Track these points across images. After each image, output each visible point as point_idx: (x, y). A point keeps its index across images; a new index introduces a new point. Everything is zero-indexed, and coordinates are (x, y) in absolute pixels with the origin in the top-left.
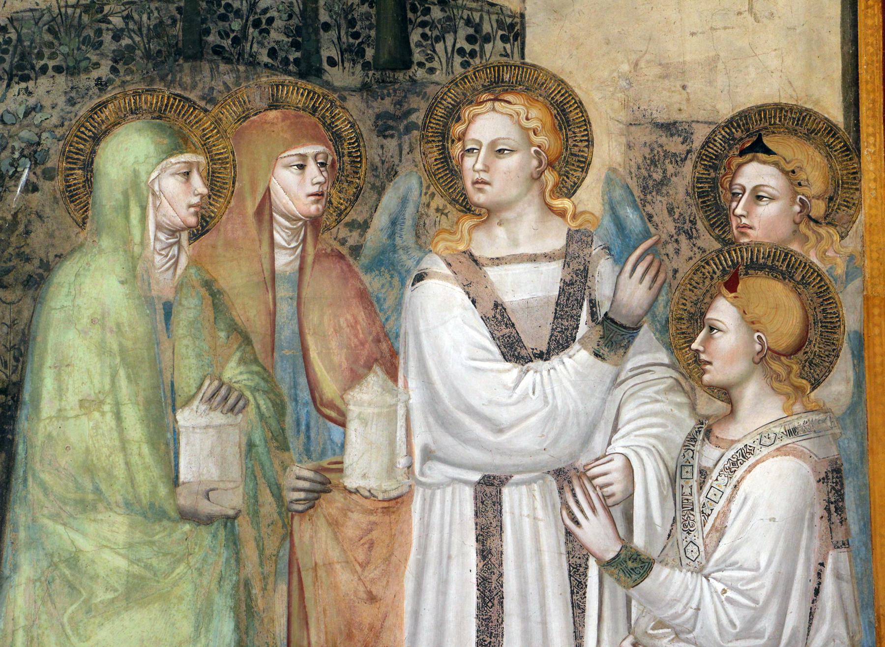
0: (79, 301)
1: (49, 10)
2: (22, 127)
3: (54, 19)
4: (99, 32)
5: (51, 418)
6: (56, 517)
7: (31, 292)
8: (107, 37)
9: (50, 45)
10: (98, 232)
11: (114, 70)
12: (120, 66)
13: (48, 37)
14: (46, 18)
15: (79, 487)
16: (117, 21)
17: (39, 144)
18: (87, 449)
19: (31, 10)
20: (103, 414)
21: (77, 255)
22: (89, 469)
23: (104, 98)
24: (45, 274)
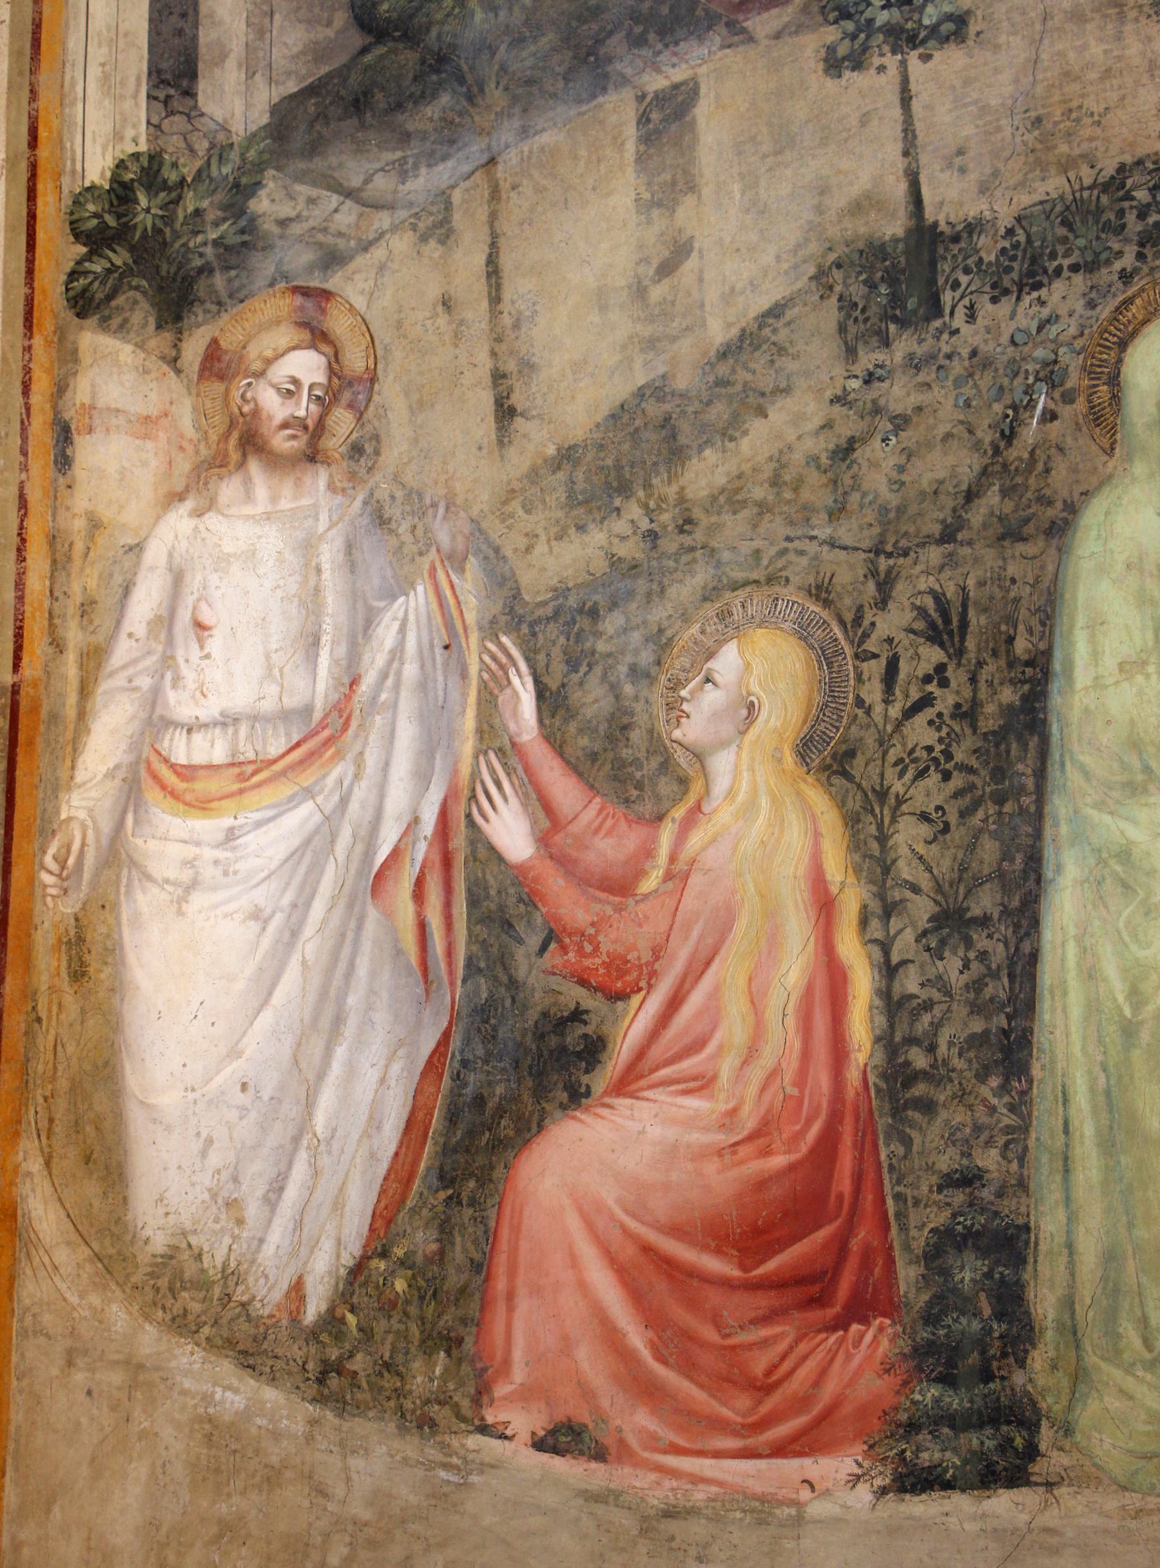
0: (1111, 545)
1: (1062, 198)
2: (1035, 346)
3: (1068, 208)
4: (1121, 213)
5: (1086, 688)
6: (1100, 806)
7: (1055, 542)
8: (1131, 217)
9: (1064, 240)
10: (1129, 458)
11: (1140, 256)
12: (1148, 251)
13: (1062, 231)
14: (1059, 208)
15: (1125, 767)
16: (1142, 195)
17: (1056, 362)
18: (1132, 722)
19: (1041, 203)
20: (1148, 676)
21: (1106, 490)
22: (1135, 744)
23: (1129, 293)
24: (1070, 517)
